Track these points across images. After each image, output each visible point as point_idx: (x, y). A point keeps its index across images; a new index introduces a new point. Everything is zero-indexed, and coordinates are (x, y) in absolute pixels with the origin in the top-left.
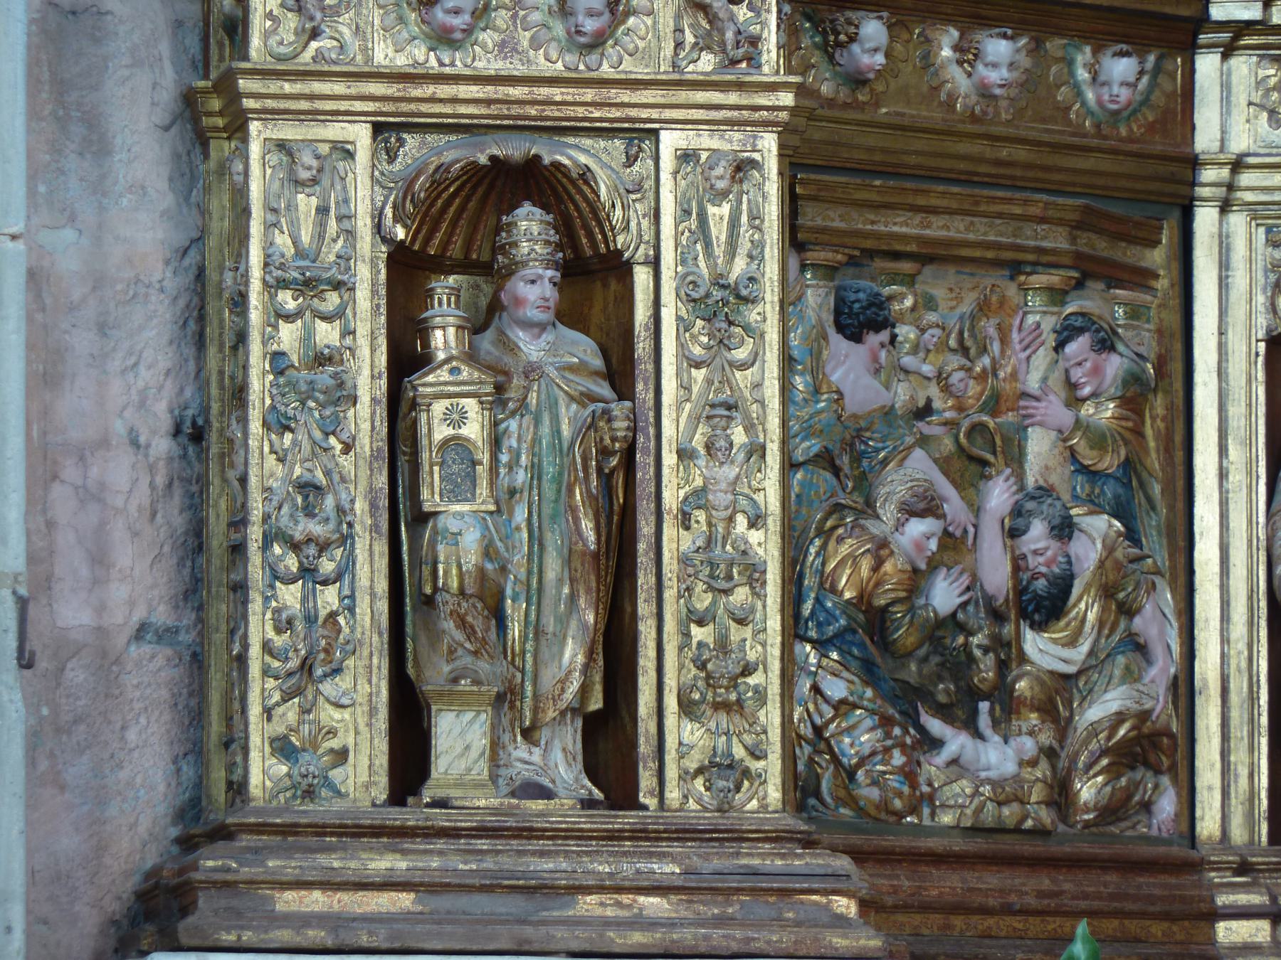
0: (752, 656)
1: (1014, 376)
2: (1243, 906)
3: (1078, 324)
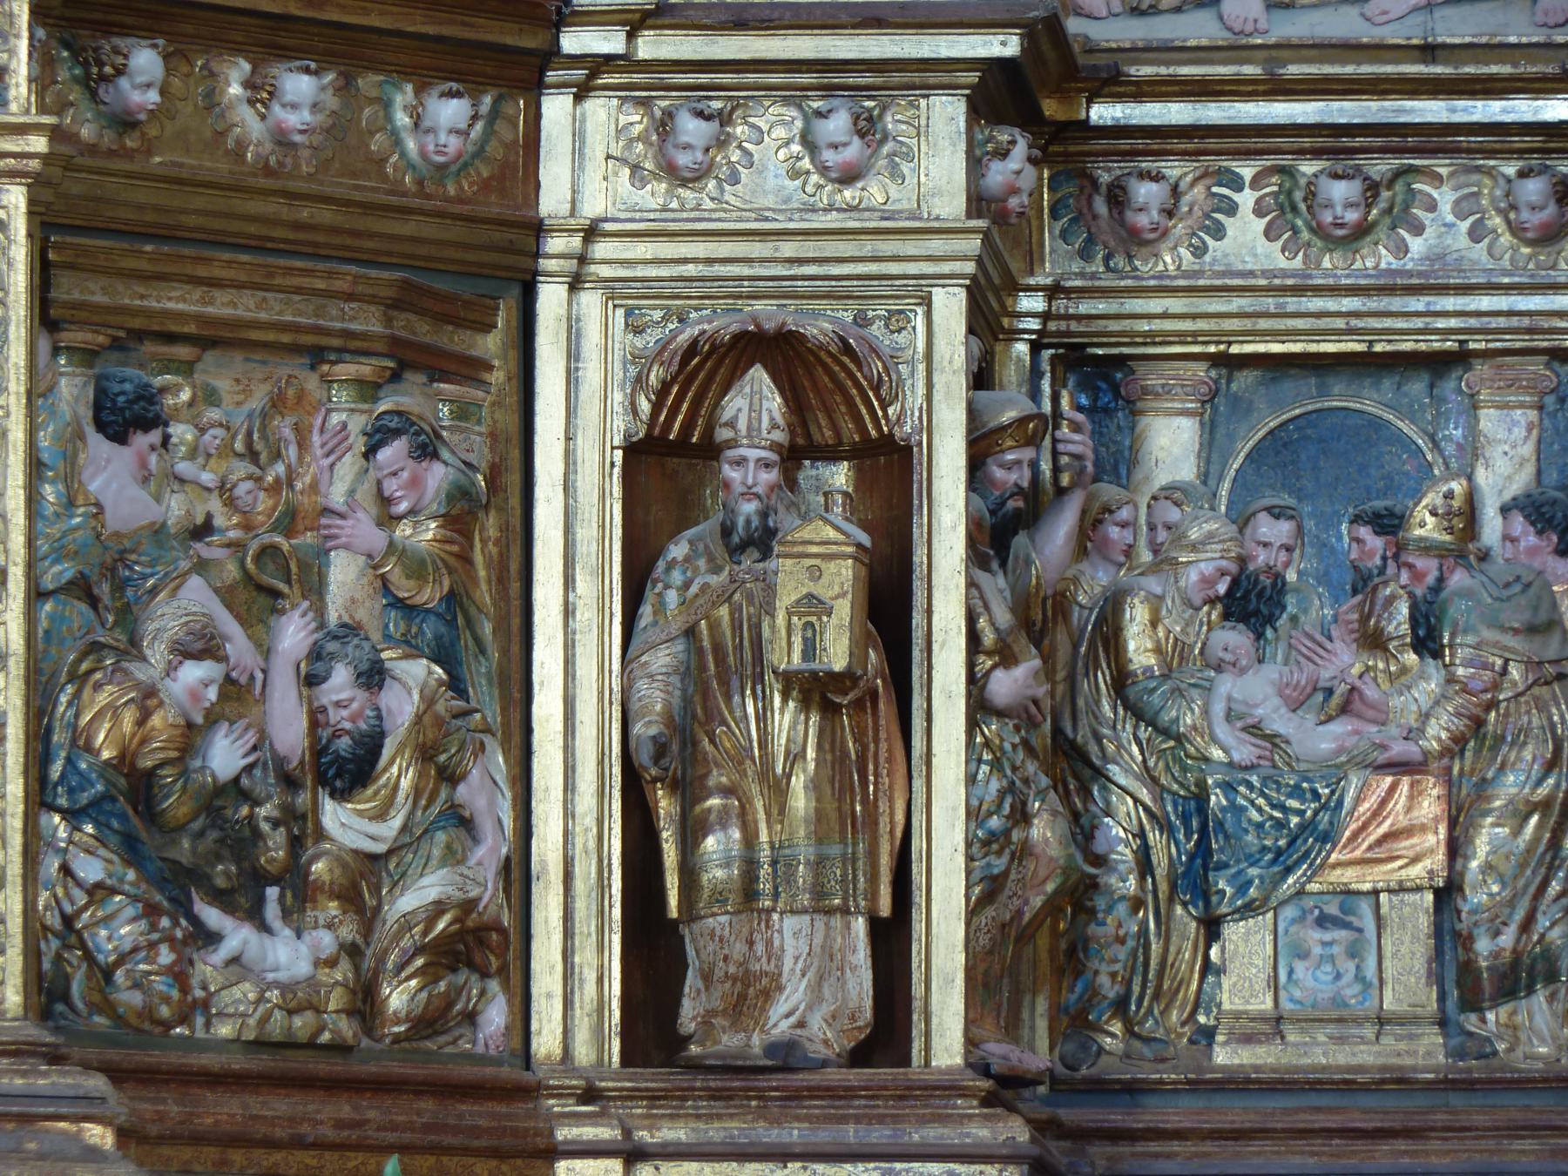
1: (314, 487)
2: (590, 1142)
3: (393, 425)
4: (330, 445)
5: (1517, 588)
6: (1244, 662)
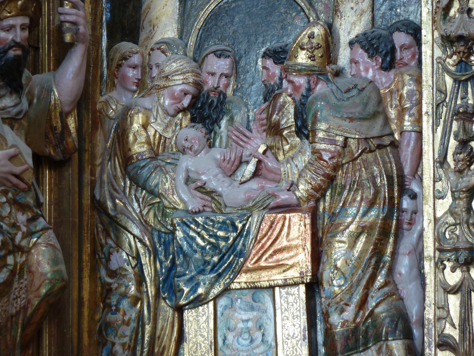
5: (354, 92)
6: (196, 147)
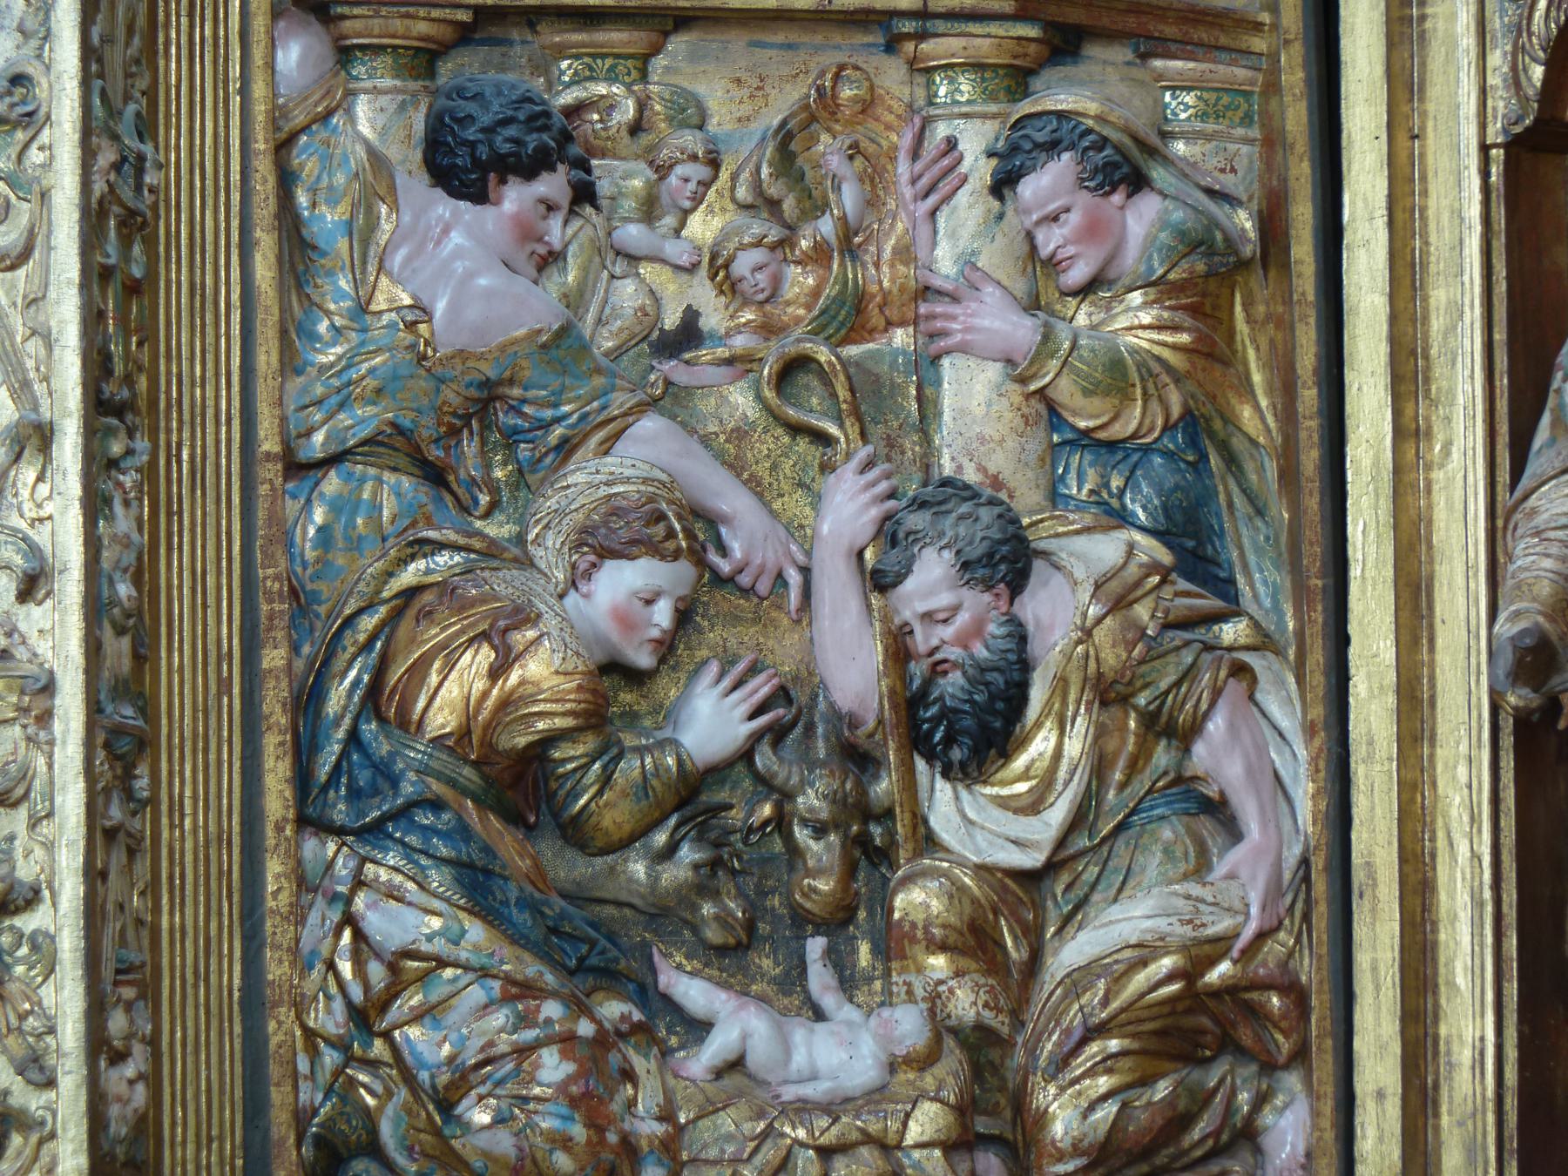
0: (26, 871)
1: (905, 253)
4: (924, 182)
